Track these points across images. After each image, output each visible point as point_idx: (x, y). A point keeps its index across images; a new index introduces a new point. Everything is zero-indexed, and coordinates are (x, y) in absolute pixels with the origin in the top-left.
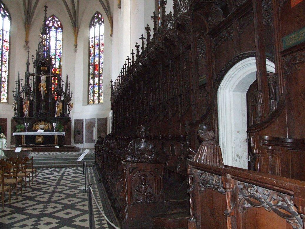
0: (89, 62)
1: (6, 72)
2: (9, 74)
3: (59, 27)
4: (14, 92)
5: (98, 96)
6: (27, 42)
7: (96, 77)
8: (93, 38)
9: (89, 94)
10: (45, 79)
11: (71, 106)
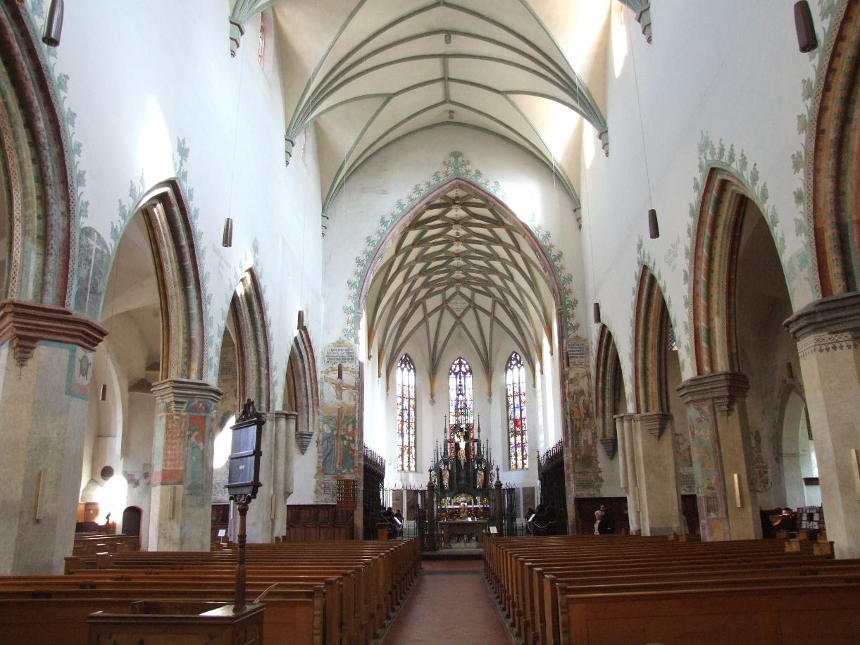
0: (508, 415)
2: (415, 437)
3: (468, 371)
6: (432, 396)
8: (512, 385)
9: (510, 457)
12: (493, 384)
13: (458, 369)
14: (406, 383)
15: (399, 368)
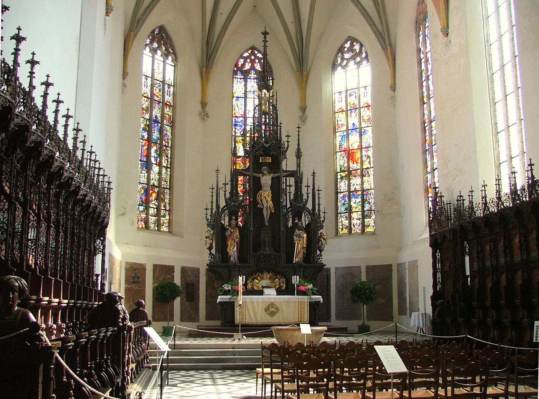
1: (167, 168)
4: (207, 209)
5: (360, 217)
6: (204, 104)
7: (355, 176)
8: (343, 94)
10: (270, 182)
11: (324, 239)
12: (309, 90)
13: (248, 66)
14: (159, 76)
15: (148, 49)
